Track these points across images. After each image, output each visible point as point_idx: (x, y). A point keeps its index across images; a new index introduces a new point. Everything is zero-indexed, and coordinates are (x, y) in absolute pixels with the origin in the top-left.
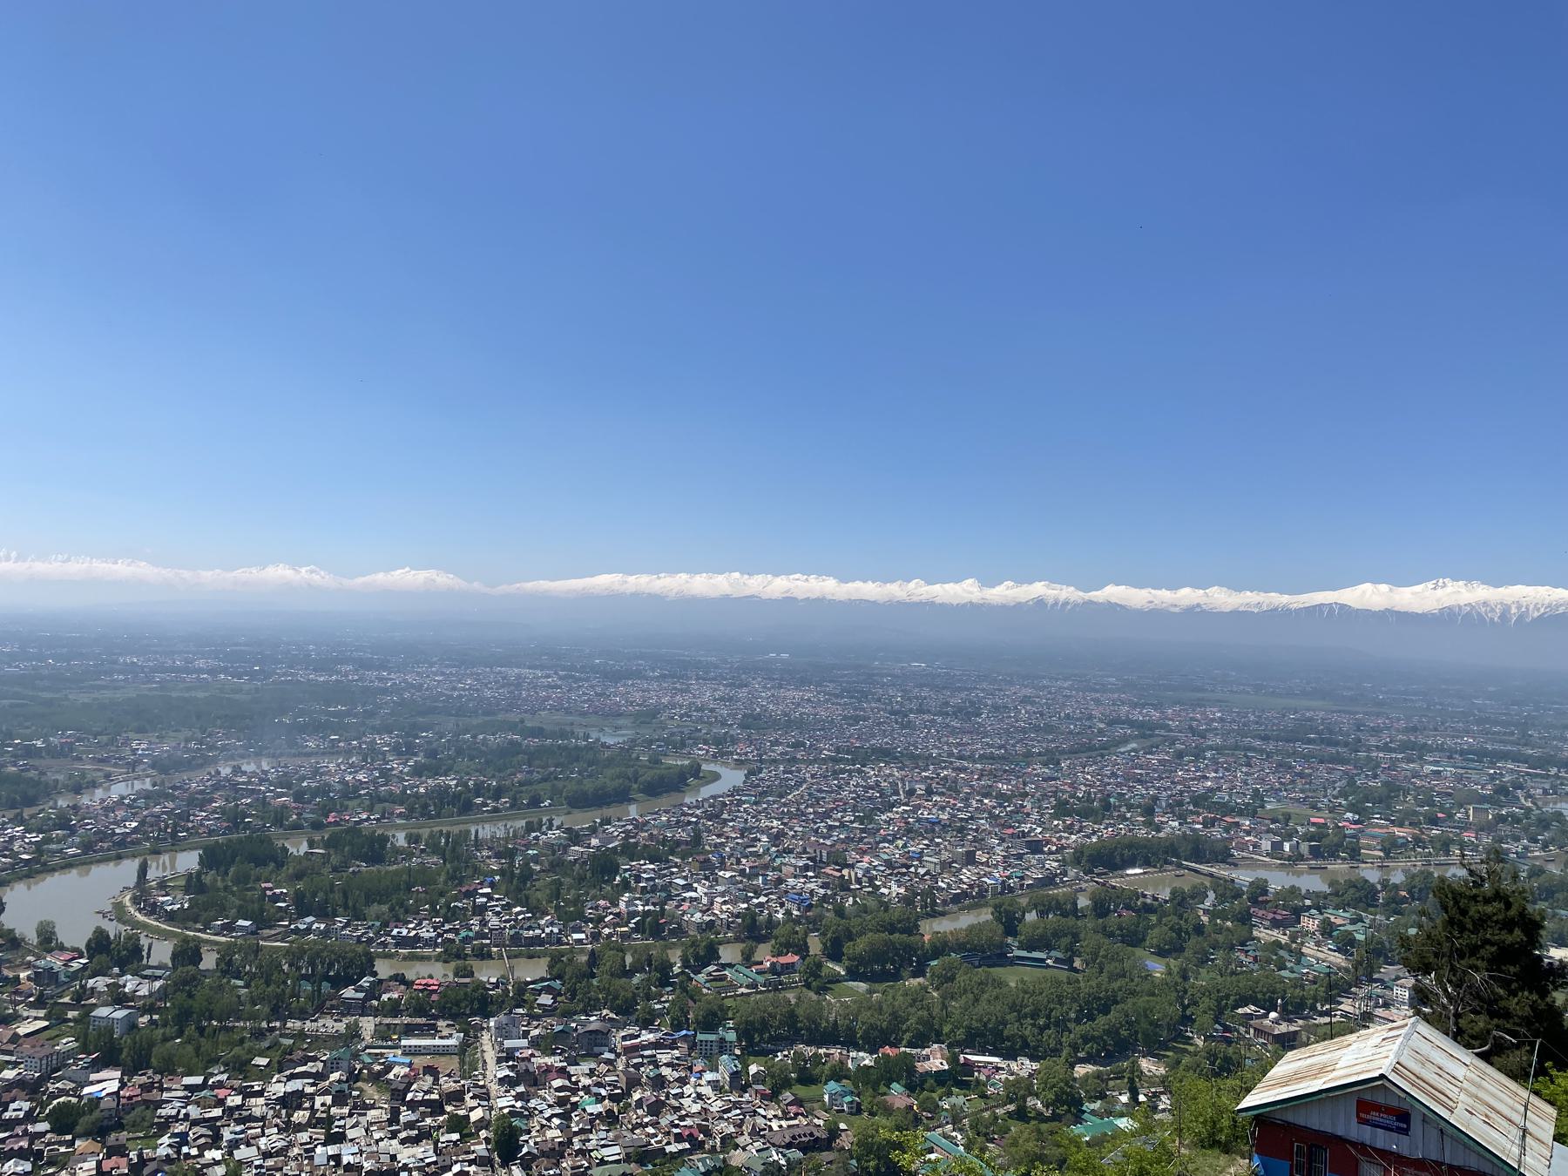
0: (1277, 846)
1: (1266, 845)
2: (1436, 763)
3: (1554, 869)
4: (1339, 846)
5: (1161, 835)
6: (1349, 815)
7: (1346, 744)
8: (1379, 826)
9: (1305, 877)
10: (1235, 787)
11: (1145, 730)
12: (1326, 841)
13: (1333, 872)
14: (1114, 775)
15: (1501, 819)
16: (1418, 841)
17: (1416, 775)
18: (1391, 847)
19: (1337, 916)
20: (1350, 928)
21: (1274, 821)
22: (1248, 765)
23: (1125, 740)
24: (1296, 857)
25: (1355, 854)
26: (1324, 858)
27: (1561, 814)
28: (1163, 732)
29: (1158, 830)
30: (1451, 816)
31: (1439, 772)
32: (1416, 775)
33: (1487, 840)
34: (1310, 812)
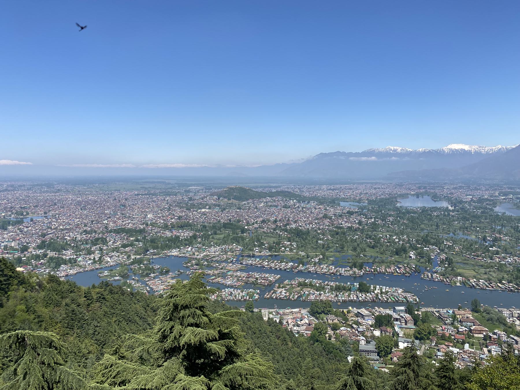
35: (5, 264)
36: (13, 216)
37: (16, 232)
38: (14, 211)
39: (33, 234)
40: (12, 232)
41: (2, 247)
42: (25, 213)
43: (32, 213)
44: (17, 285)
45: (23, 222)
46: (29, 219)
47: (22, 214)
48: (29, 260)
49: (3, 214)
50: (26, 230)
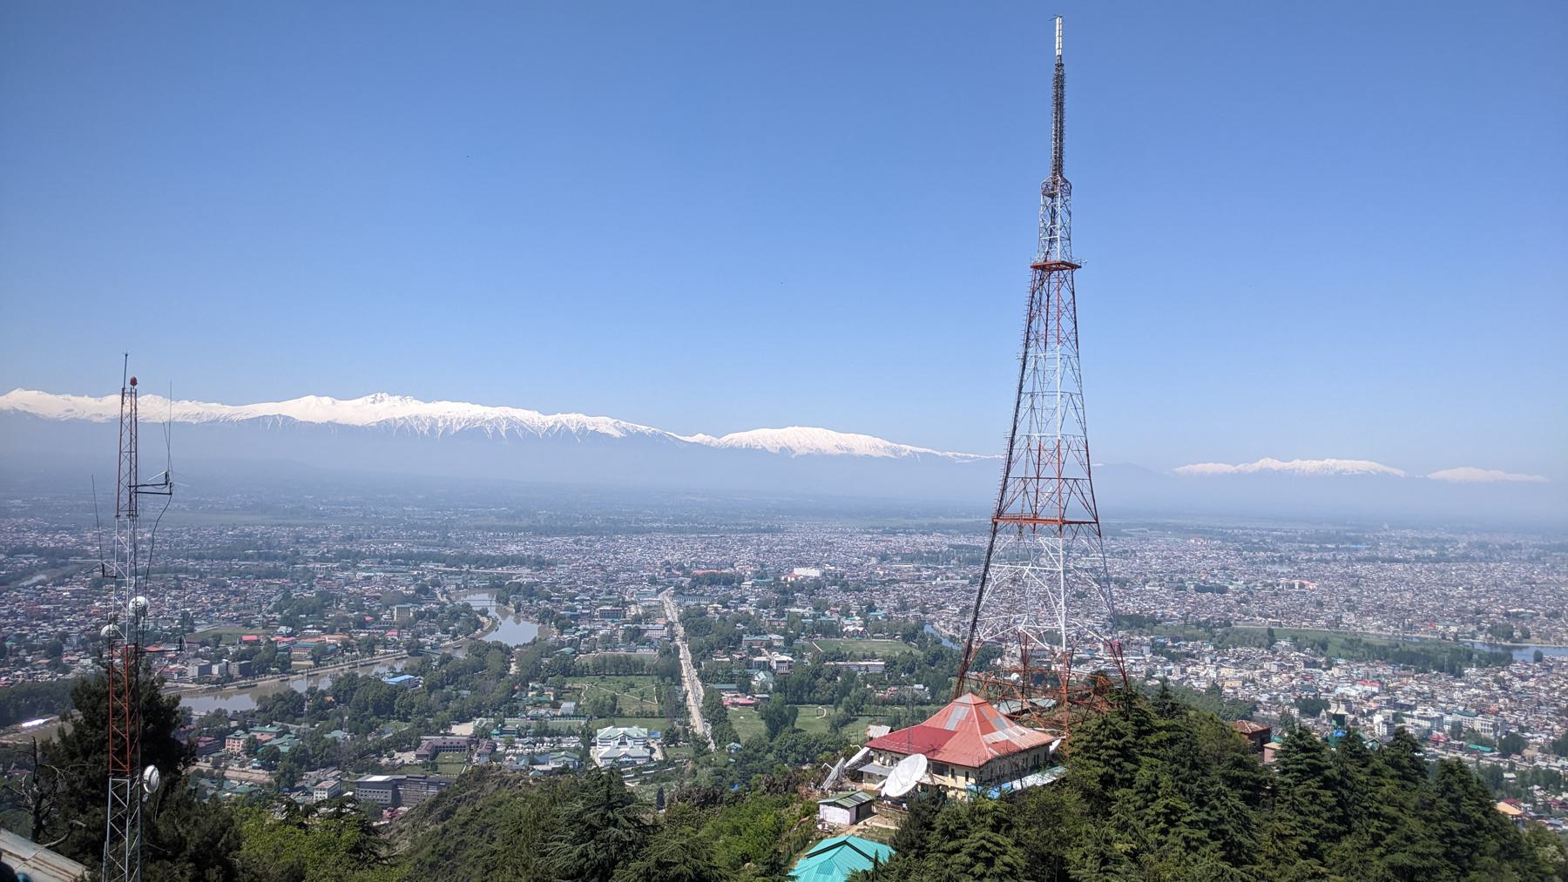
0: (205, 671)
1: (193, 671)
2: (368, 569)
3: (461, 655)
4: (270, 661)
5: (70, 676)
6: (283, 629)
7: (284, 558)
8: (313, 635)
9: (235, 697)
10: (161, 613)
11: (56, 559)
12: (256, 658)
13: (264, 688)
14: (13, 614)
15: (420, 616)
16: (346, 646)
17: (349, 582)
18: (320, 656)
19: (262, 733)
20: (275, 742)
21: (203, 644)
22: (178, 587)
23: (30, 571)
24: (227, 678)
25: (286, 667)
26: (254, 676)
27: (468, 605)
28: (79, 559)
29: (66, 670)
30: (377, 618)
31: (369, 578)
32: (349, 582)
33: (407, 636)
34: (243, 630)
35: (1465, 783)
36: (1481, 637)
37: (1488, 688)
38: (1485, 624)
39: (1540, 704)
40: (1478, 685)
41: (1447, 728)
42: (1517, 634)
43: (1540, 635)
44: (1496, 855)
45: (1511, 661)
46: (1532, 652)
47: (1509, 636)
48: (1524, 785)
49: (1454, 629)
50: (1518, 685)
